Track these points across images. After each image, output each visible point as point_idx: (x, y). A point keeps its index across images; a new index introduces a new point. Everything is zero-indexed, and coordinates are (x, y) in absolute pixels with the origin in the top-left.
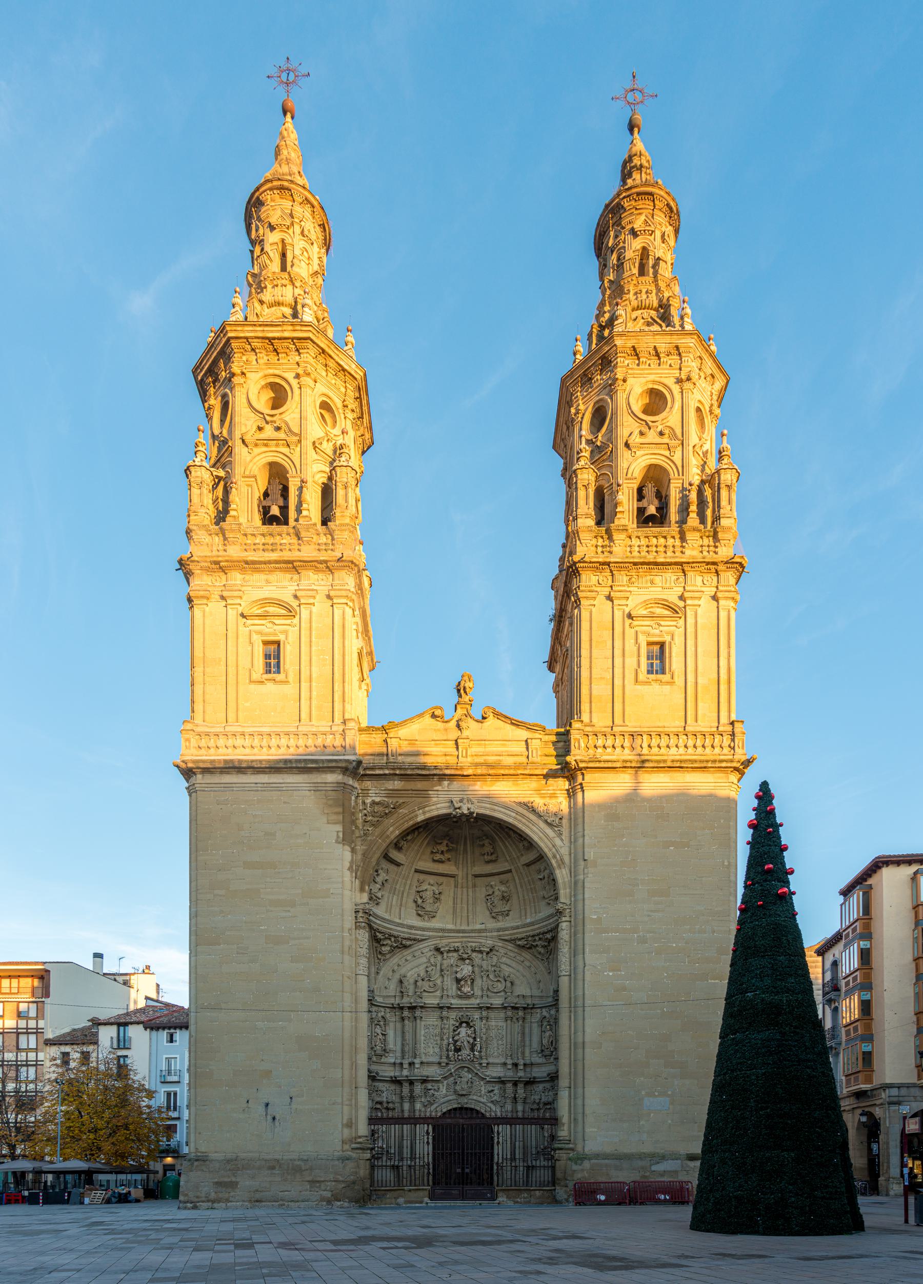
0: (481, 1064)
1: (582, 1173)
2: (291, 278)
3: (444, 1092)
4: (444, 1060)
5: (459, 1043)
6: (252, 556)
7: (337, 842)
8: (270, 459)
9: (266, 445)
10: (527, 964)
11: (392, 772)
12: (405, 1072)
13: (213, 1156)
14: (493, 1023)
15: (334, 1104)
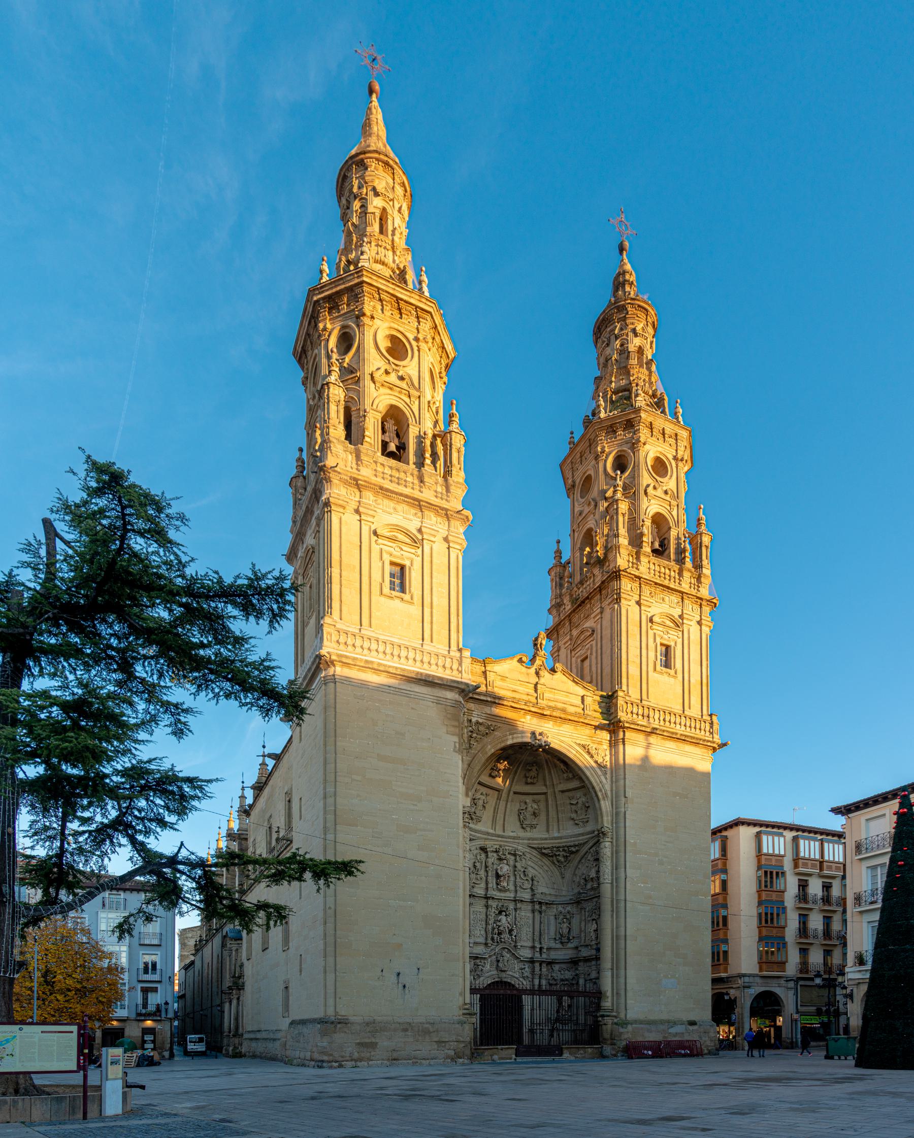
1: (628, 1035)
2: (394, 246)
4: (489, 941)
5: (501, 928)
6: (387, 485)
7: (454, 751)
8: (394, 403)
9: (391, 389)
10: (546, 868)
11: (493, 700)
13: (352, 1019)
15: (453, 975)
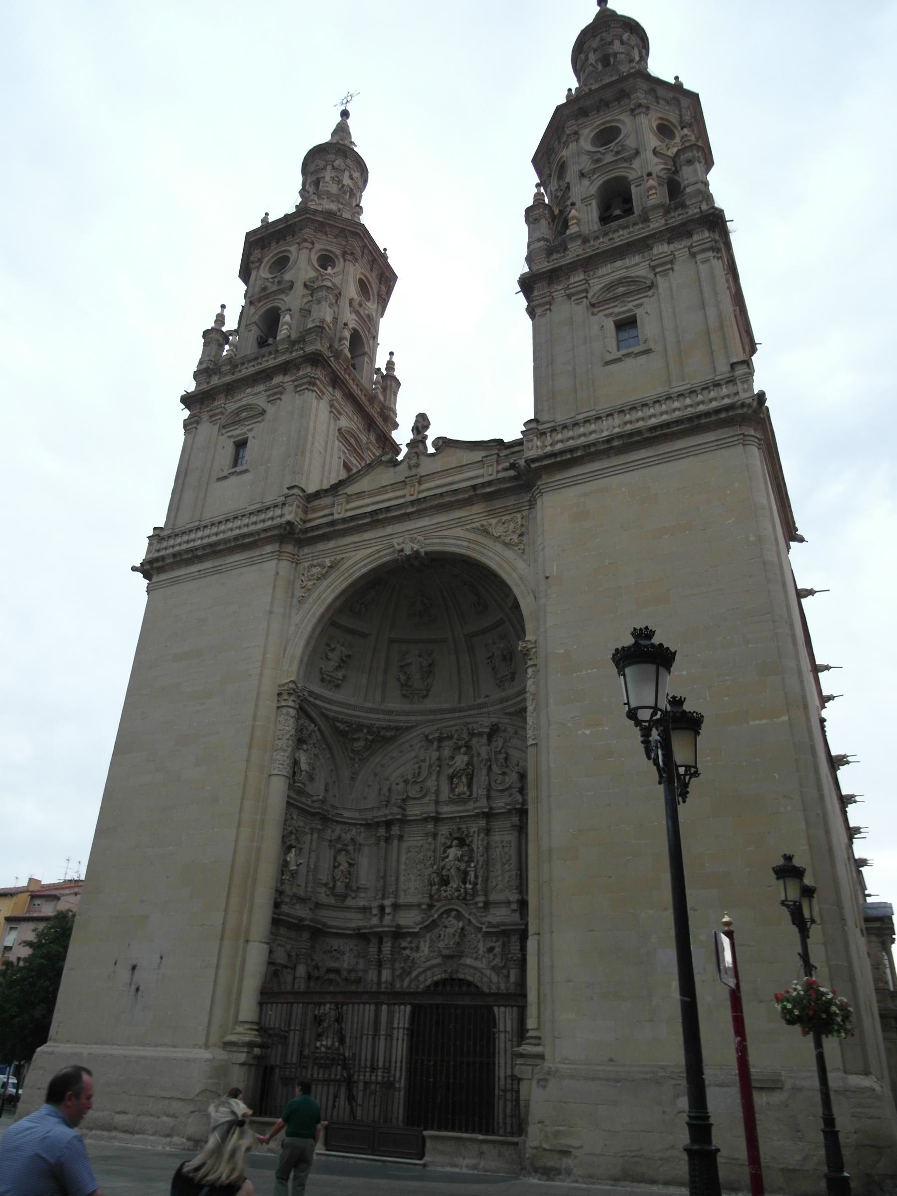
0: (476, 903)
3: (426, 951)
12: (375, 921)
14: (496, 837)
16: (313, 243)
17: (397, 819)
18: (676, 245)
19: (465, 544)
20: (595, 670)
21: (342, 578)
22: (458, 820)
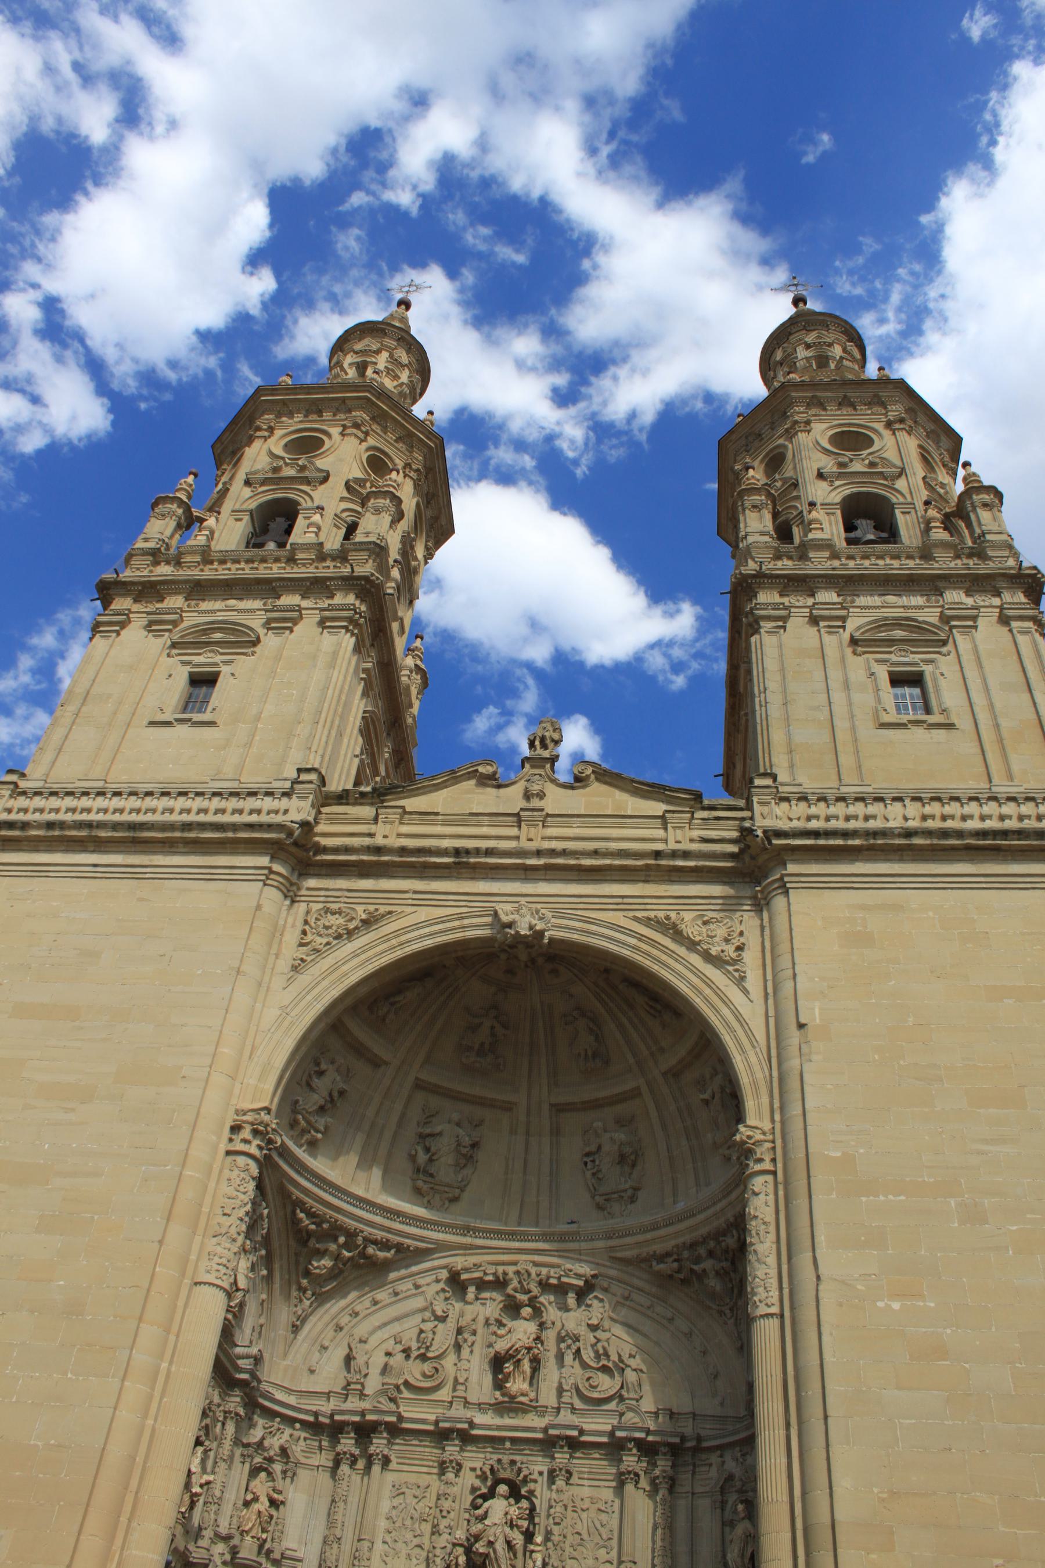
16: (367, 434)
17: (387, 1423)
18: (980, 600)
19: (633, 941)
20: (902, 1198)
21: (385, 946)
22: (508, 1444)
